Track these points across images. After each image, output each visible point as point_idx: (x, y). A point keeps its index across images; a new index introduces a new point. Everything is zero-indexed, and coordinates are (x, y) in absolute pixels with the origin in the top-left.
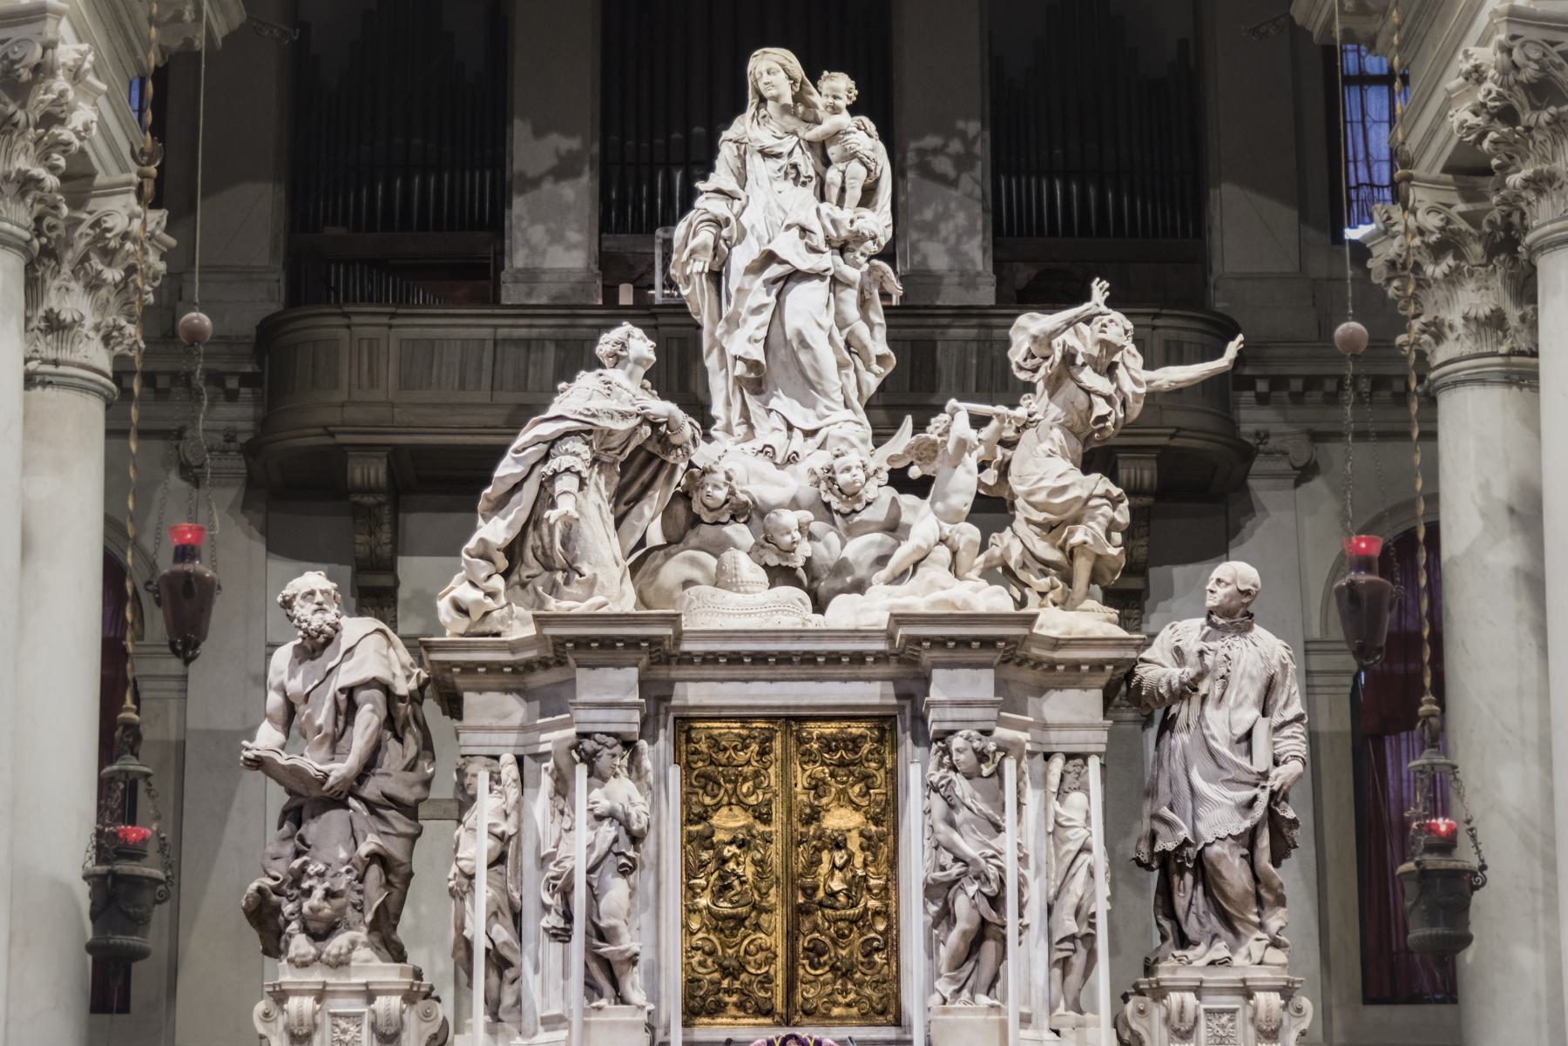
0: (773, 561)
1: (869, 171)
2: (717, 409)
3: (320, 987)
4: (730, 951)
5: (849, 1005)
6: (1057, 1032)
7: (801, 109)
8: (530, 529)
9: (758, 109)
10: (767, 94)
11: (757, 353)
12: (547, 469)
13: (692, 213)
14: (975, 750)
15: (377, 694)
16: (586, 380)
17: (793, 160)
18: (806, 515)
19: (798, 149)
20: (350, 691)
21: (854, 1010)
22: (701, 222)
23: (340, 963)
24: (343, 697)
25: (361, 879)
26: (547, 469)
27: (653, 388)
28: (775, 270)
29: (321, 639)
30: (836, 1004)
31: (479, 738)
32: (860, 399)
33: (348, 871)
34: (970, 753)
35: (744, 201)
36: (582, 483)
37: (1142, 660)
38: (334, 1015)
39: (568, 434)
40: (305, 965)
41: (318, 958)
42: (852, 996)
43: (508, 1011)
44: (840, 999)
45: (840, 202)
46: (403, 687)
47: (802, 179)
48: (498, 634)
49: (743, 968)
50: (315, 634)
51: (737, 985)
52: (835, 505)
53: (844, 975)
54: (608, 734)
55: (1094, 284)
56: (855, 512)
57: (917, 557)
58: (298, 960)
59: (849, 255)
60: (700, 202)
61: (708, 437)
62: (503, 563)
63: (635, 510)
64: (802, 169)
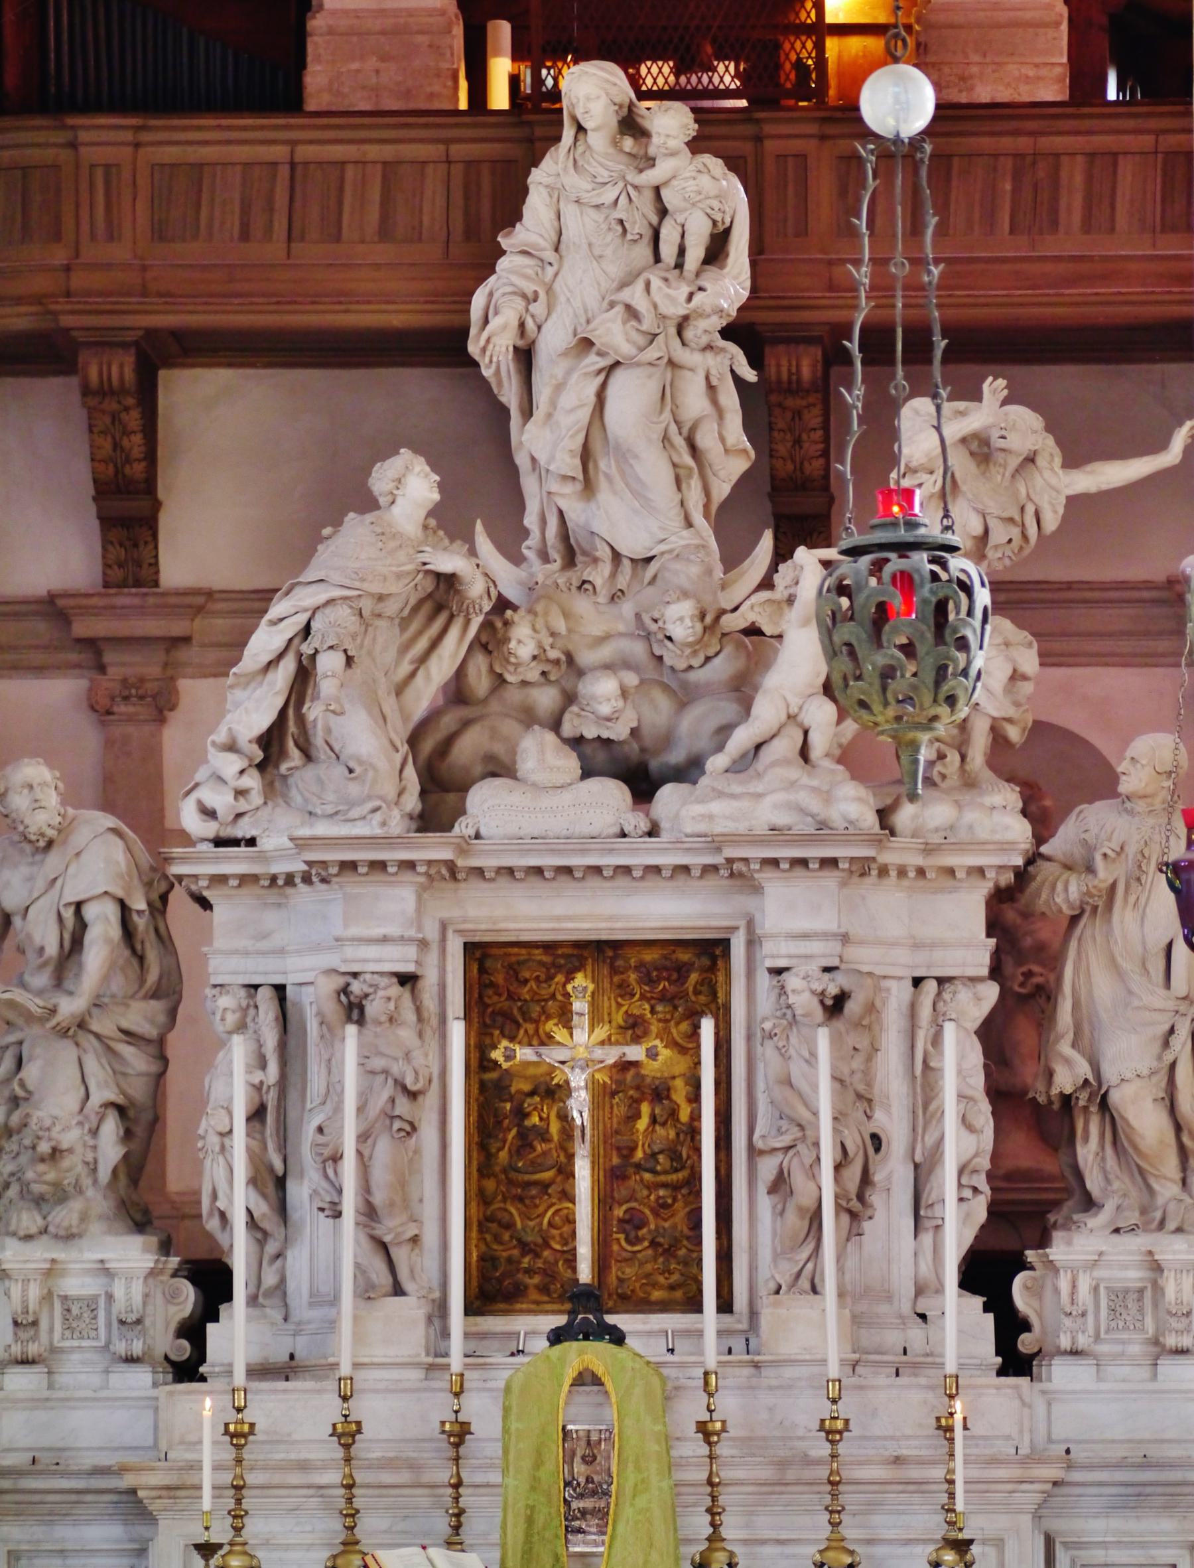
0: (590, 733)
1: (715, 223)
2: (530, 520)
3: (48, 1266)
4: (531, 1224)
5: (672, 1288)
6: (923, 1317)
7: (628, 143)
8: (291, 712)
9: (576, 139)
10: (585, 125)
11: (572, 466)
12: (306, 649)
13: (492, 279)
14: (813, 992)
15: (111, 911)
16: (356, 527)
17: (619, 214)
18: (631, 679)
19: (623, 200)
20: (79, 906)
21: (678, 1294)
22: (504, 294)
23: (69, 1237)
24: (69, 914)
25: (95, 1132)
26: (306, 649)
27: (440, 526)
28: (593, 361)
29: (42, 844)
30: (655, 1285)
31: (234, 963)
32: (706, 515)
33: (80, 1124)
34: (807, 995)
35: (556, 267)
36: (349, 661)
37: (1041, 856)
38: (65, 1298)
39: (330, 602)
40: (28, 1238)
41: (44, 1231)
42: (675, 1278)
43: (269, 1294)
44: (661, 1279)
45: (679, 266)
46: (139, 903)
47: (629, 237)
48: (252, 842)
49: (546, 1245)
50: (33, 838)
51: (540, 1264)
52: (668, 661)
53: (666, 1251)
54: (381, 974)
55: (986, 386)
56: (691, 667)
57: (760, 740)
58: (22, 1233)
59: (689, 334)
60: (503, 264)
61: (517, 559)
62: (259, 755)
63: (421, 673)
64: (627, 225)
